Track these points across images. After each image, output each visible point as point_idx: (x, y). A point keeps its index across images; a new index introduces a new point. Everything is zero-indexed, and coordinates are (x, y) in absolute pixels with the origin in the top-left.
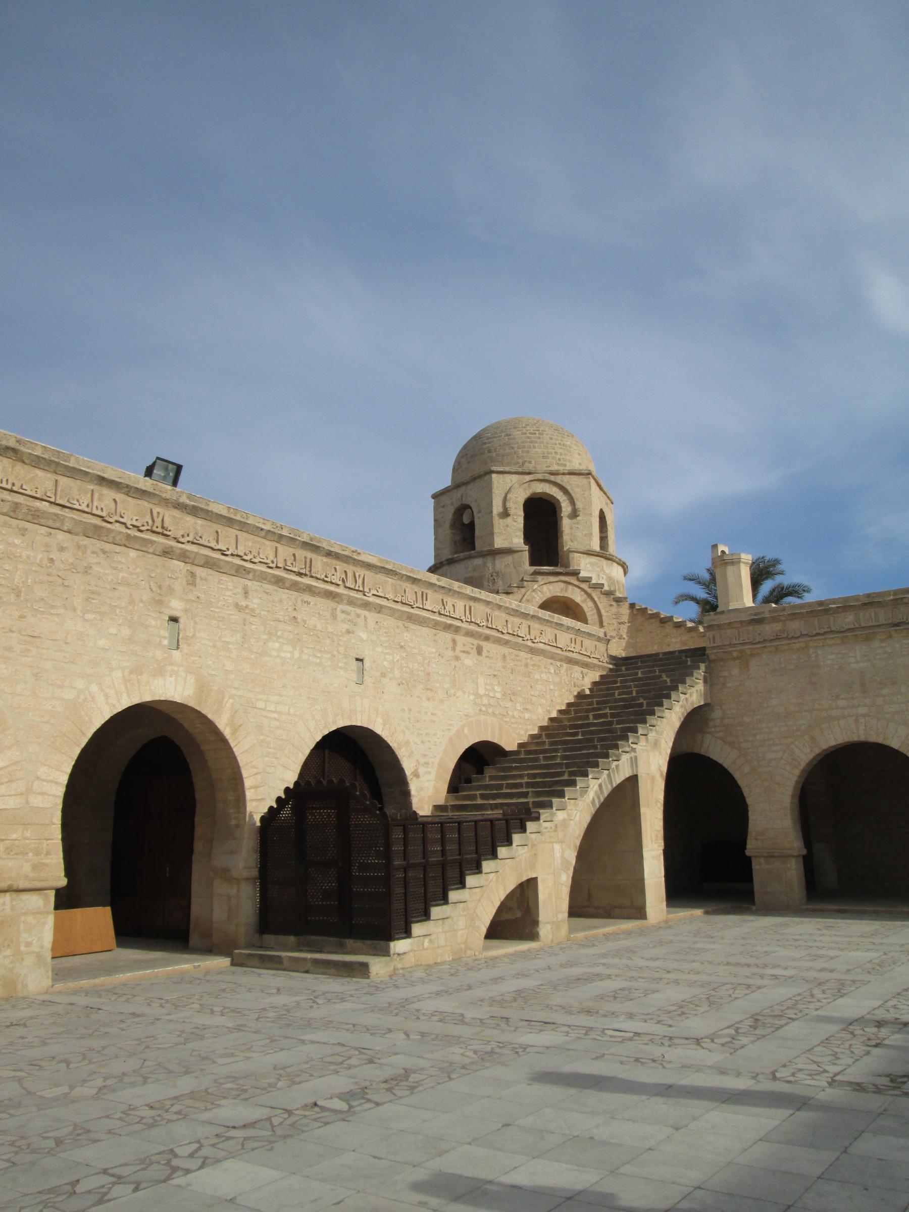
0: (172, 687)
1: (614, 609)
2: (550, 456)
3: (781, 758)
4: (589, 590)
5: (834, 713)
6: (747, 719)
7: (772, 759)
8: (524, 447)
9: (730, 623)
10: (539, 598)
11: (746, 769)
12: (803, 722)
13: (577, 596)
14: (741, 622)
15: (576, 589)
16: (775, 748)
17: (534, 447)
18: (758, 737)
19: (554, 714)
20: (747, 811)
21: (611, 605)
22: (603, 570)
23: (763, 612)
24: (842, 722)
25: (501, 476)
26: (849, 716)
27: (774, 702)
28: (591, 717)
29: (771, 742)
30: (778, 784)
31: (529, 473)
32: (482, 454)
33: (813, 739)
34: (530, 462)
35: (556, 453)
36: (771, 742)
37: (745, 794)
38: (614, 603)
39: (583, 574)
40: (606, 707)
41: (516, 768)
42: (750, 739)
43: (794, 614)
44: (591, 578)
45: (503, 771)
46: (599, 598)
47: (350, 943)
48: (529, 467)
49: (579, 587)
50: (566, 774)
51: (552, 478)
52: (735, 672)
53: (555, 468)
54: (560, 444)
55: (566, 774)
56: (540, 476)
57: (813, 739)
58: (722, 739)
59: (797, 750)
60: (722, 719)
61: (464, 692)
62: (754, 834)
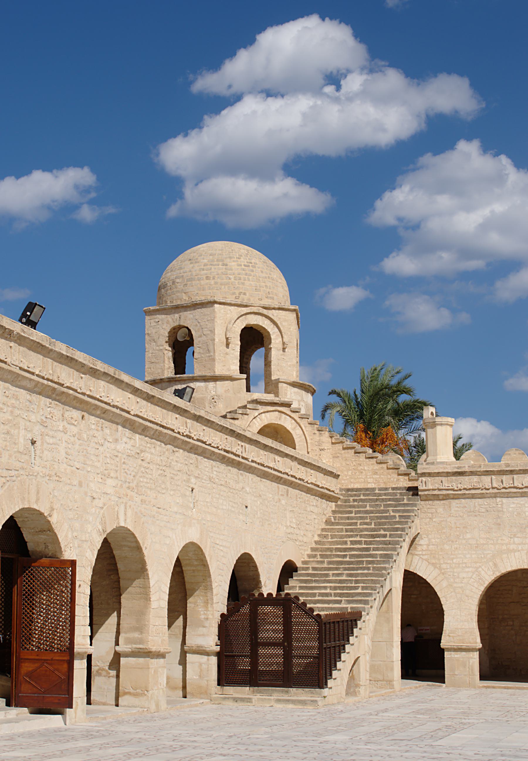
0: (193, 535)
1: (317, 437)
2: (262, 289)
3: (471, 578)
4: (298, 420)
5: (512, 547)
8: (240, 279)
9: (439, 473)
10: (258, 425)
11: (445, 584)
12: (489, 552)
13: (288, 424)
14: (448, 473)
15: (288, 417)
16: (467, 570)
17: (249, 280)
18: (454, 561)
19: (317, 538)
20: (443, 615)
21: (314, 433)
23: (464, 467)
24: (516, 554)
25: (222, 306)
26: (522, 550)
27: (468, 536)
28: (349, 543)
29: (464, 565)
30: (467, 596)
31: (246, 306)
32: (199, 280)
33: (495, 565)
34: (245, 294)
35: (266, 286)
36: (464, 565)
37: (442, 603)
40: (357, 535)
41: (315, 581)
42: (449, 562)
43: (487, 471)
44: (300, 409)
45: (305, 583)
46: (305, 427)
47: (293, 690)
49: (290, 417)
50: (360, 588)
51: (265, 312)
52: (440, 510)
54: (269, 277)
55: (360, 588)
56: (255, 309)
57: (495, 565)
58: (427, 560)
59: (483, 573)
60: (428, 545)
61: (282, 525)
62: (447, 632)
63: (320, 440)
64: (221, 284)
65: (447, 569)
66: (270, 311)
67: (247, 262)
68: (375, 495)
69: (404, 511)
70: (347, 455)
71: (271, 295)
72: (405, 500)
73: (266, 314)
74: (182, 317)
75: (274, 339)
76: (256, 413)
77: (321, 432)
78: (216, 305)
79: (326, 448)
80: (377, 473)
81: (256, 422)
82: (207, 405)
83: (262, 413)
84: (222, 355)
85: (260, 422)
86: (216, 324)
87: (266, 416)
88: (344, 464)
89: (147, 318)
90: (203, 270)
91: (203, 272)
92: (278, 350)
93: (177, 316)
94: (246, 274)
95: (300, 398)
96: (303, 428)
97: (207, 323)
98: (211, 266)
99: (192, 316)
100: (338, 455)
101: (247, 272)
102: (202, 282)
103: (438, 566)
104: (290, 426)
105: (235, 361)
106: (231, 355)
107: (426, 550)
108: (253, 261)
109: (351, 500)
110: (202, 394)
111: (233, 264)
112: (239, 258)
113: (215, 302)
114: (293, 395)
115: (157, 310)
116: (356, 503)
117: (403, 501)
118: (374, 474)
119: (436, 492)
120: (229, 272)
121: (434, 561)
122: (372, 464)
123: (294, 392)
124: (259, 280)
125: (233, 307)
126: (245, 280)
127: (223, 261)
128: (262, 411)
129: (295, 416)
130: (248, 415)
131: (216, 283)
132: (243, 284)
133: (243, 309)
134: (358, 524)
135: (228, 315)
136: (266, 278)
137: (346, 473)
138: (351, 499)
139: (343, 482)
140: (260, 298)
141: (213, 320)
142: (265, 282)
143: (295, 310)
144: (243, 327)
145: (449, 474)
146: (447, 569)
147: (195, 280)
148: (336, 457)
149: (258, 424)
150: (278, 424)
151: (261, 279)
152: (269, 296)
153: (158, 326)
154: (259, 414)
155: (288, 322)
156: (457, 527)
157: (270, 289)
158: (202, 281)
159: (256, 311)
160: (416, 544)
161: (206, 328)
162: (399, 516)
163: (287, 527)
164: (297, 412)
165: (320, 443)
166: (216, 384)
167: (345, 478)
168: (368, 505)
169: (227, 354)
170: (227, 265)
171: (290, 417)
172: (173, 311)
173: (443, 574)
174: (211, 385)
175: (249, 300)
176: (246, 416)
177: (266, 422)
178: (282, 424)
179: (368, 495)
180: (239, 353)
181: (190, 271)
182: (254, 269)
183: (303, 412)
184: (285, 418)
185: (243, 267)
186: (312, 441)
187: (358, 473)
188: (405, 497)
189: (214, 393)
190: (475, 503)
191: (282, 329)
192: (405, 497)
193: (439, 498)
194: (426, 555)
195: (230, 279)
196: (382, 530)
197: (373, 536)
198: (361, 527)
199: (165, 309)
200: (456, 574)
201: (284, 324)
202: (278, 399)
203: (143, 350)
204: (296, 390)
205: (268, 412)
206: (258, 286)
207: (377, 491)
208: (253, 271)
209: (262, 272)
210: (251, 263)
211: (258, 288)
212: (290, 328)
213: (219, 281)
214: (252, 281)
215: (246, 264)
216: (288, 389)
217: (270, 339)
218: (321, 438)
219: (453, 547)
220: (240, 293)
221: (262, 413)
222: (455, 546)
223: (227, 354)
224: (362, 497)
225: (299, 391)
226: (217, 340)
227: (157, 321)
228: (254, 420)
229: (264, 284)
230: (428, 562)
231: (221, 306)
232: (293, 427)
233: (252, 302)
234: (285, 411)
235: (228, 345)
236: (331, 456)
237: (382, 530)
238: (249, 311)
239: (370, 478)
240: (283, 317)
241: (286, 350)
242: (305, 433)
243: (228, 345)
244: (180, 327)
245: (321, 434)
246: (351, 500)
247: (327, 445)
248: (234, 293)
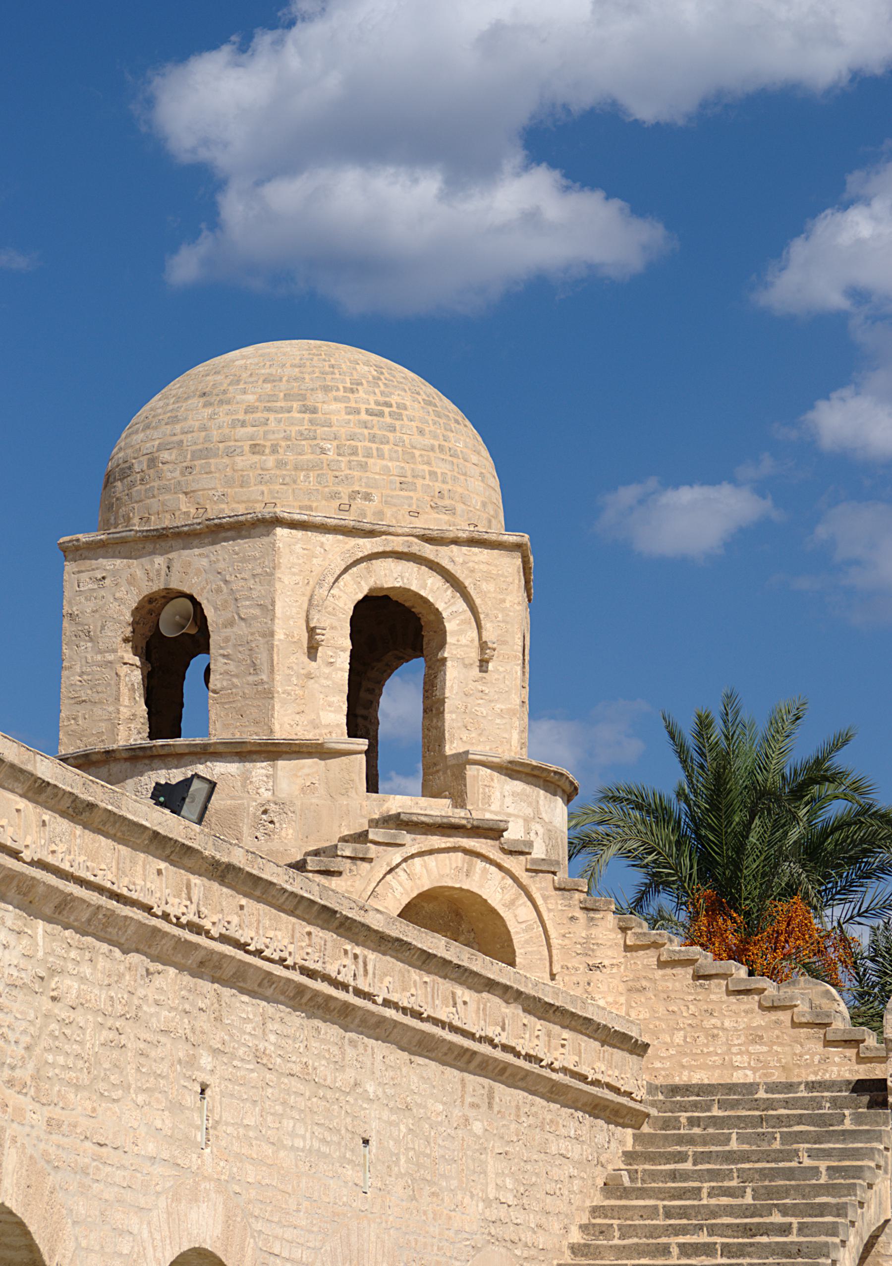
1: (580, 930)
2: (419, 482)
4: (524, 877)
8: (355, 453)
13: (491, 887)
15: (493, 869)
17: (381, 456)
19: (576, 1237)
21: (572, 918)
22: (537, 811)
25: (299, 534)
28: (675, 1251)
31: (371, 534)
32: (230, 453)
34: (367, 497)
35: (433, 474)
38: (579, 914)
39: (514, 833)
40: (701, 1227)
44: (530, 844)
46: (545, 898)
48: (365, 513)
49: (500, 867)
51: (428, 551)
53: (434, 522)
56: (397, 544)
61: (472, 1196)
63: (588, 937)
64: (296, 468)
66: (443, 550)
67: (377, 403)
68: (756, 1104)
69: (845, 1154)
70: (670, 985)
71: (447, 502)
72: (847, 1121)
73: (431, 557)
74: (176, 566)
75: (454, 633)
76: (396, 856)
77: (592, 914)
78: (279, 531)
80: (761, 1037)
81: (394, 883)
82: (245, 830)
83: (412, 856)
84: (294, 680)
85: (408, 884)
86: (278, 585)
87: (425, 866)
88: (661, 1010)
89: (70, 567)
90: (243, 424)
91: (241, 432)
92: (466, 666)
93: (159, 561)
94: (373, 439)
95: (529, 811)
96: (540, 902)
97: (251, 583)
98: (266, 415)
99: (204, 562)
100: (644, 983)
101: (376, 431)
102: (240, 462)
104: (499, 896)
106: (324, 682)
108: (394, 399)
109: (683, 1121)
110: (232, 798)
111: (334, 406)
112: (352, 391)
113: (278, 522)
114: (508, 801)
115: (102, 544)
116: (696, 1130)
117: (842, 1122)
118: (754, 1042)
120: (320, 431)
122: (746, 1012)
123: (514, 794)
124: (413, 457)
125: (330, 537)
126: (369, 455)
127: (304, 398)
128: (414, 850)
129: (515, 864)
130: (370, 860)
131: (281, 464)
133: (361, 541)
134: (705, 1193)
135: (315, 561)
136: (432, 449)
137: (668, 1040)
138: (683, 1116)
139: (658, 1065)
140: (414, 508)
141: (268, 576)
142: (429, 463)
143: (518, 547)
144: (360, 596)
147: (216, 455)
148: (638, 990)
149: (400, 889)
150: (461, 889)
151: (417, 453)
152: (440, 503)
153: (102, 593)
154: (405, 860)
155: (498, 581)
157: (444, 482)
158: (238, 459)
159: (400, 549)
160: (879, 1254)
161: (248, 598)
162: (829, 1168)
163: (487, 1202)
164: (522, 853)
165: (588, 947)
166: (273, 767)
167: (663, 1054)
168: (734, 1136)
169: (309, 676)
171: (500, 867)
172: (150, 547)
174: (260, 769)
175: (380, 514)
176: (366, 866)
177: (426, 885)
179: (734, 1105)
180: (346, 675)
181: (204, 428)
182: (398, 423)
183: (539, 852)
184: (484, 870)
185: (364, 416)
186: (567, 942)
187: (702, 1040)
188: (847, 1112)
189: (268, 795)
191: (478, 601)
192: (847, 1112)
195: (323, 451)
196: (775, 1211)
197: (749, 1231)
198: (713, 1201)
199: (123, 541)
201: (484, 586)
202: (462, 813)
203: (56, 663)
204: (518, 786)
205: (431, 852)
206: (409, 473)
207: (761, 1094)
208: (393, 429)
209: (421, 432)
210: (388, 405)
211: (409, 479)
212: (504, 601)
213: (291, 457)
214: (391, 459)
215: (373, 406)
216: (495, 783)
217: (442, 633)
218: (593, 931)
220: (353, 495)
221: (412, 856)
223: (309, 676)
224: (716, 1112)
225: (528, 789)
226: (279, 635)
227: (99, 577)
228: (389, 877)
229: (426, 467)
231: (294, 531)
232: (508, 897)
233: (388, 520)
234: (483, 851)
235: (312, 651)
236: (622, 988)
237: (775, 1211)
238: (381, 549)
239: (740, 1053)
240: (484, 567)
241: (491, 666)
242: (545, 917)
243: (312, 651)
244: (170, 595)
245: (592, 919)
246: (683, 1121)
247: (610, 953)
248: (335, 495)
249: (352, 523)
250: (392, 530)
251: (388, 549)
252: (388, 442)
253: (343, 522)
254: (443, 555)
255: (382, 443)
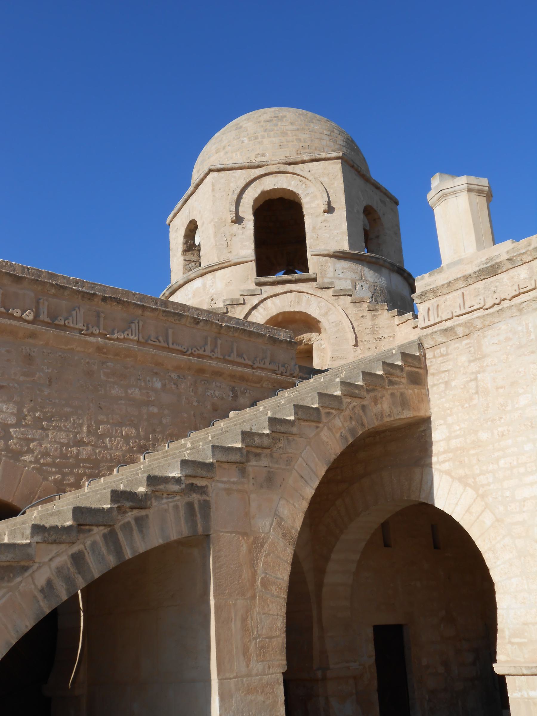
6: (484, 436)
7: (525, 500)
11: (488, 519)
17: (269, 137)
18: (502, 462)
29: (522, 470)
31: (258, 167)
36: (522, 470)
56: (274, 169)
60: (448, 439)
62: (507, 633)
63: (373, 326)
65: (489, 484)
79: (385, 336)
103: (471, 481)
105: (247, 243)
107: (445, 452)
114: (339, 272)
119: (449, 324)
121: (461, 472)
126: (263, 137)
132: (261, 143)
145: (470, 281)
146: (489, 484)
156: (497, 388)
170: (241, 127)
173: (483, 497)
178: (302, 310)
185: (262, 123)
190: (527, 325)
193: (455, 333)
194: (444, 462)
200: (508, 494)
214: (275, 137)
218: (377, 322)
219: (495, 432)
222: (500, 429)
230: (452, 477)
238: (264, 173)
249: (248, 164)
250: (269, 163)
251: (267, 172)
252: (273, 131)
253: (242, 164)
254: (297, 169)
255: (270, 131)
